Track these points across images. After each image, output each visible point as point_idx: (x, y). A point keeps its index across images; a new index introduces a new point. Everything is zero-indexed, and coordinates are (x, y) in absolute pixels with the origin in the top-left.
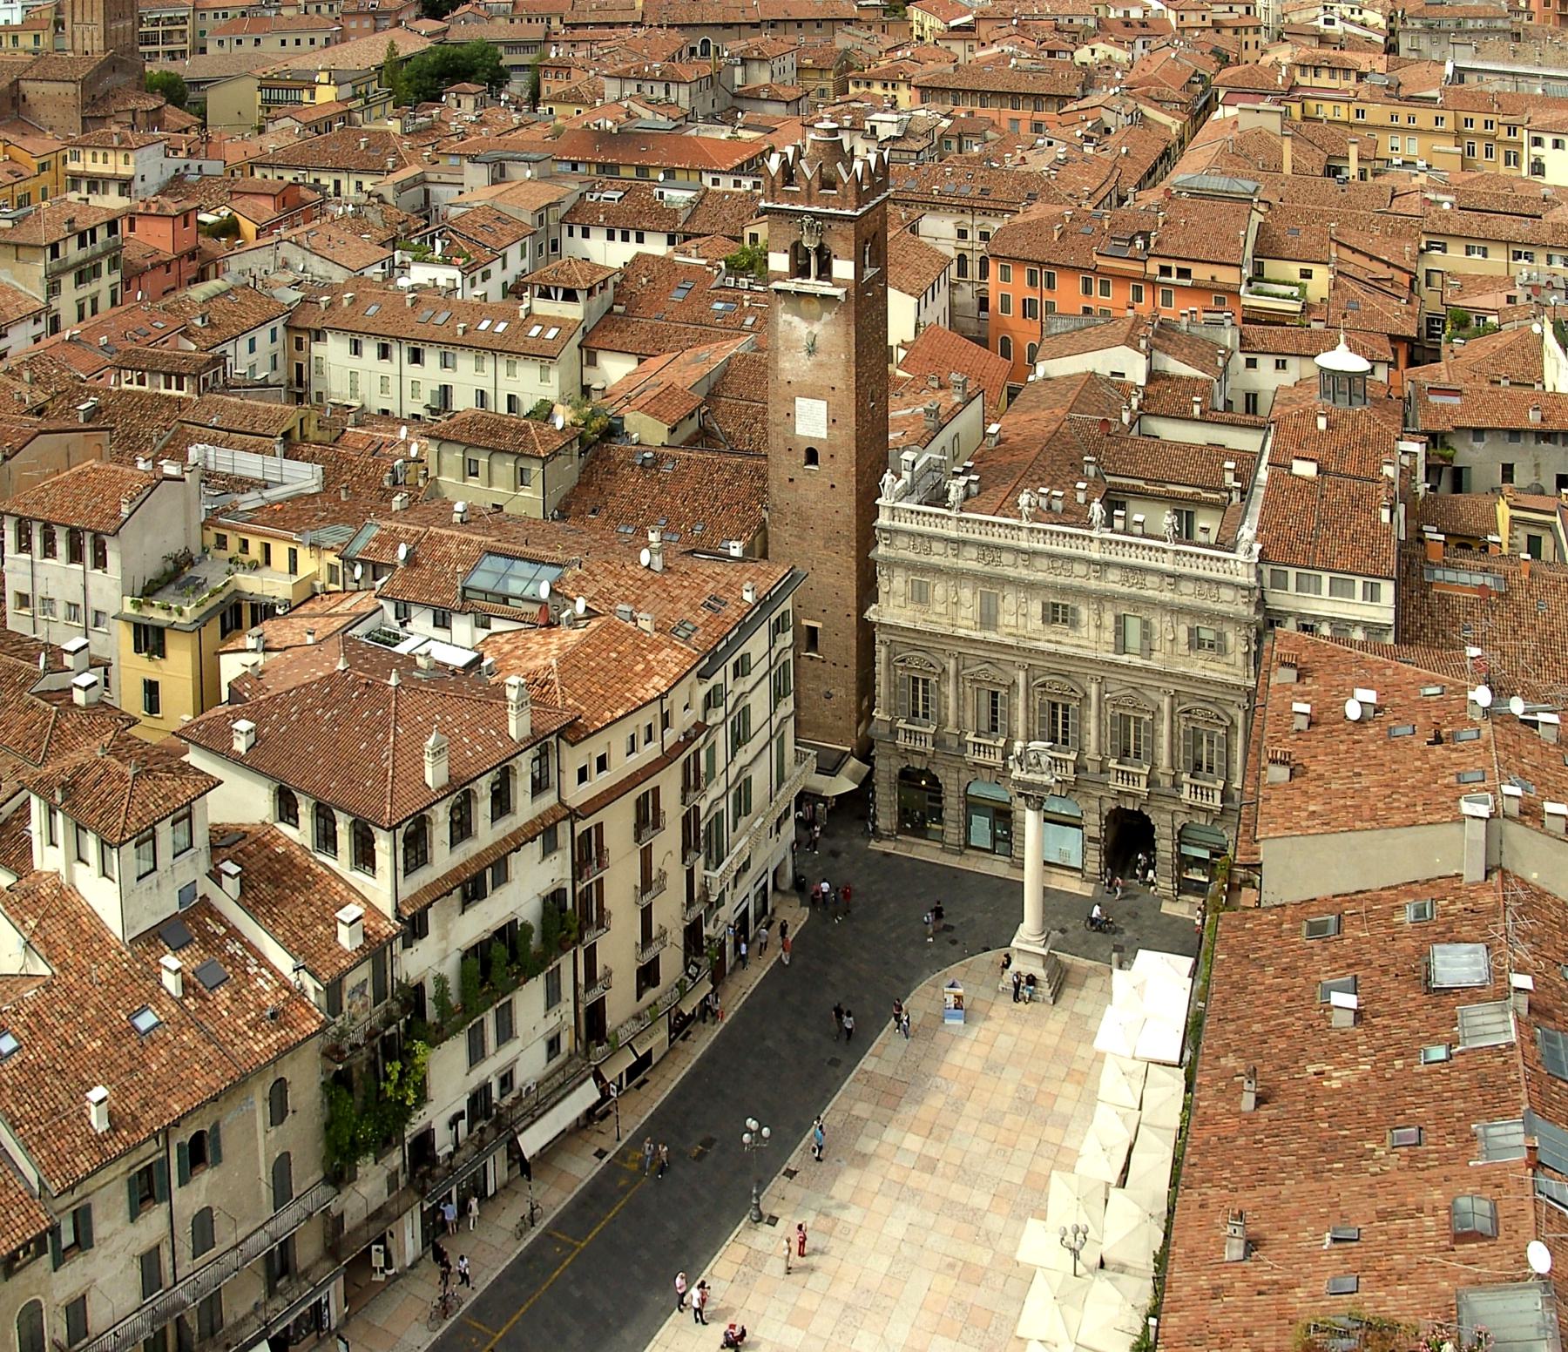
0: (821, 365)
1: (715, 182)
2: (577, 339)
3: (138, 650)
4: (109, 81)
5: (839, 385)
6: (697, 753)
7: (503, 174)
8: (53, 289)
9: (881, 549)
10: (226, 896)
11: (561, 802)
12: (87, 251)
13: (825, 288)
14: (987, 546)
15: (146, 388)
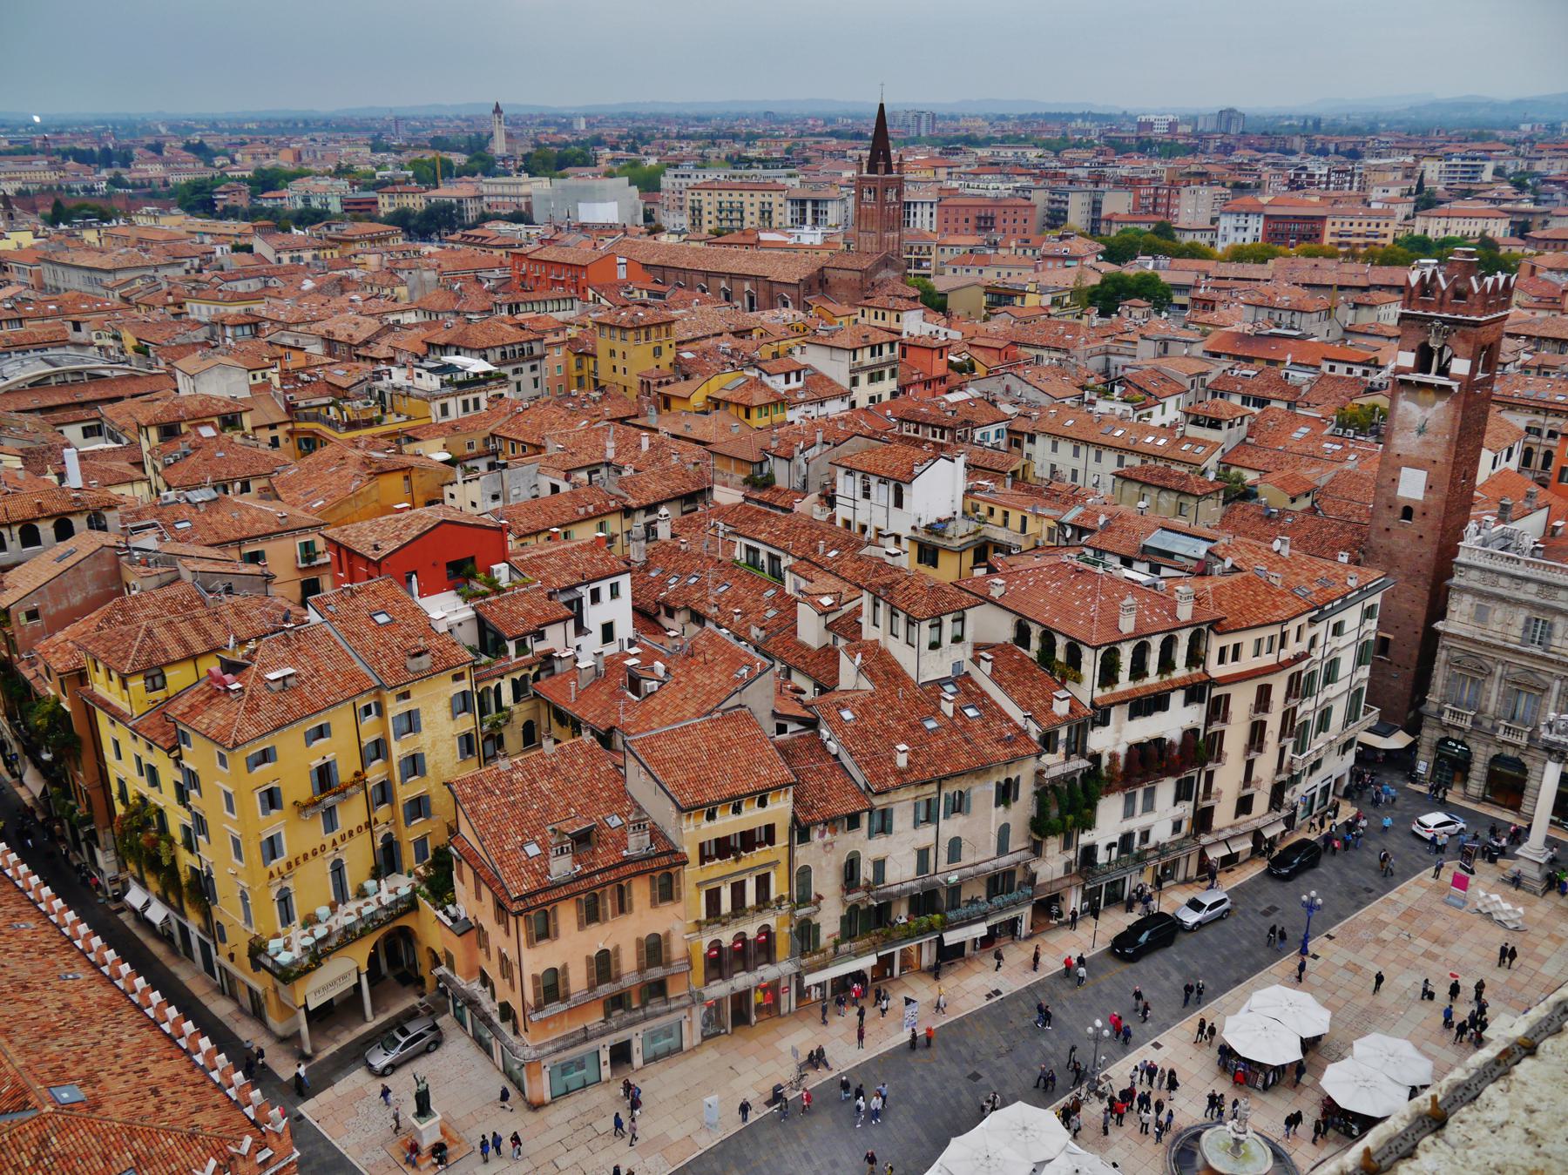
0: (1427, 443)
1: (1332, 369)
2: (1217, 455)
3: (920, 561)
4: (882, 275)
5: (1440, 458)
6: (1300, 673)
7: (1166, 351)
8: (854, 382)
9: (1456, 580)
10: (982, 675)
11: (1205, 671)
12: (877, 360)
13: (1443, 381)
14: (1548, 584)
15: (919, 436)
